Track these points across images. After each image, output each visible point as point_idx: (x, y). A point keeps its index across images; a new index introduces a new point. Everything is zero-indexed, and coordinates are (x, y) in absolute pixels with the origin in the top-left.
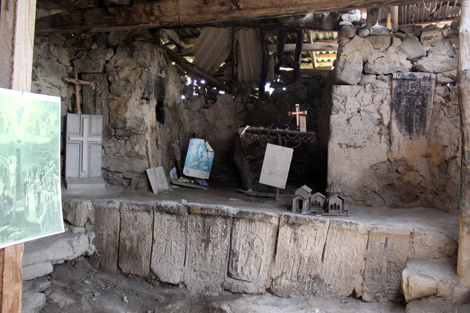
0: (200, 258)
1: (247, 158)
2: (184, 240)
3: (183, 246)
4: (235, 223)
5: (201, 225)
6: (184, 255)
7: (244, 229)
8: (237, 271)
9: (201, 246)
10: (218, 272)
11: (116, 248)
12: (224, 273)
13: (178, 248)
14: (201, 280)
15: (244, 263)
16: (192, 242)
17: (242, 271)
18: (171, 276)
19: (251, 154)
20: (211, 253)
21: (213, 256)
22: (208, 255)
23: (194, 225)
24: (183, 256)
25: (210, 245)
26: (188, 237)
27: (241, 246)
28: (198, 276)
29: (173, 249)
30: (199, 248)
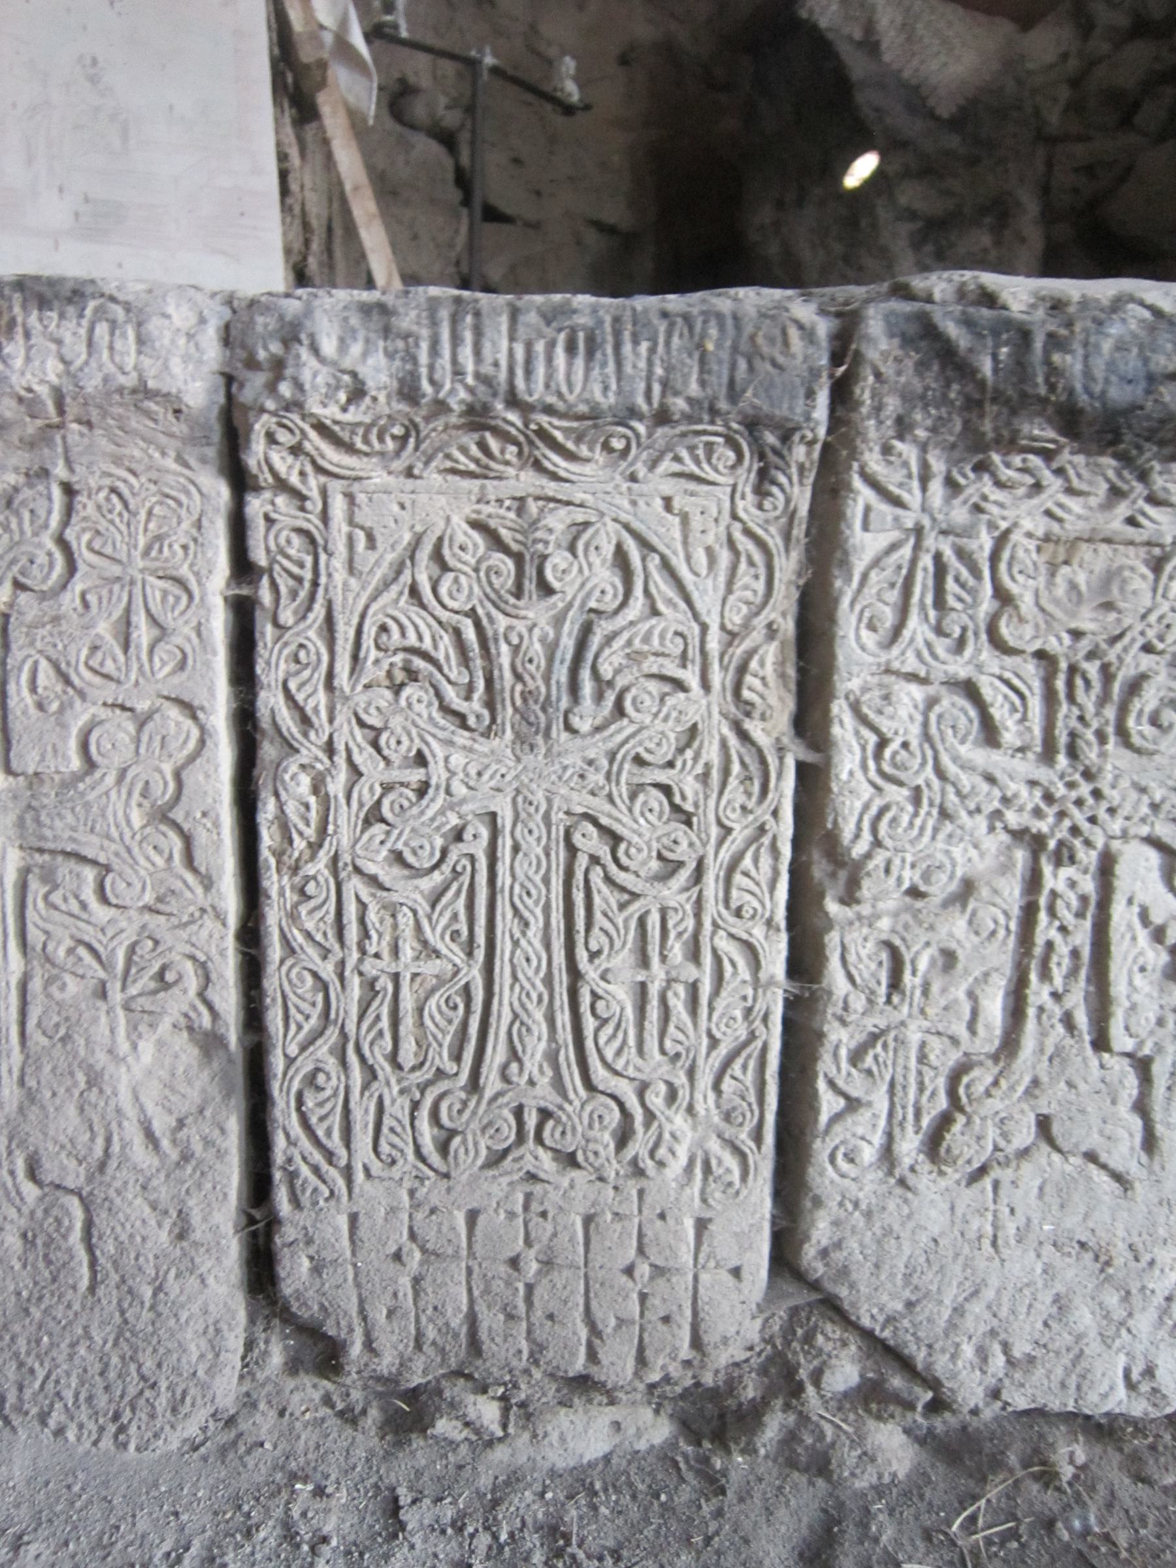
1: (903, 200)
11: (210, 1043)
18: (1114, 1328)
29: (1135, 960)
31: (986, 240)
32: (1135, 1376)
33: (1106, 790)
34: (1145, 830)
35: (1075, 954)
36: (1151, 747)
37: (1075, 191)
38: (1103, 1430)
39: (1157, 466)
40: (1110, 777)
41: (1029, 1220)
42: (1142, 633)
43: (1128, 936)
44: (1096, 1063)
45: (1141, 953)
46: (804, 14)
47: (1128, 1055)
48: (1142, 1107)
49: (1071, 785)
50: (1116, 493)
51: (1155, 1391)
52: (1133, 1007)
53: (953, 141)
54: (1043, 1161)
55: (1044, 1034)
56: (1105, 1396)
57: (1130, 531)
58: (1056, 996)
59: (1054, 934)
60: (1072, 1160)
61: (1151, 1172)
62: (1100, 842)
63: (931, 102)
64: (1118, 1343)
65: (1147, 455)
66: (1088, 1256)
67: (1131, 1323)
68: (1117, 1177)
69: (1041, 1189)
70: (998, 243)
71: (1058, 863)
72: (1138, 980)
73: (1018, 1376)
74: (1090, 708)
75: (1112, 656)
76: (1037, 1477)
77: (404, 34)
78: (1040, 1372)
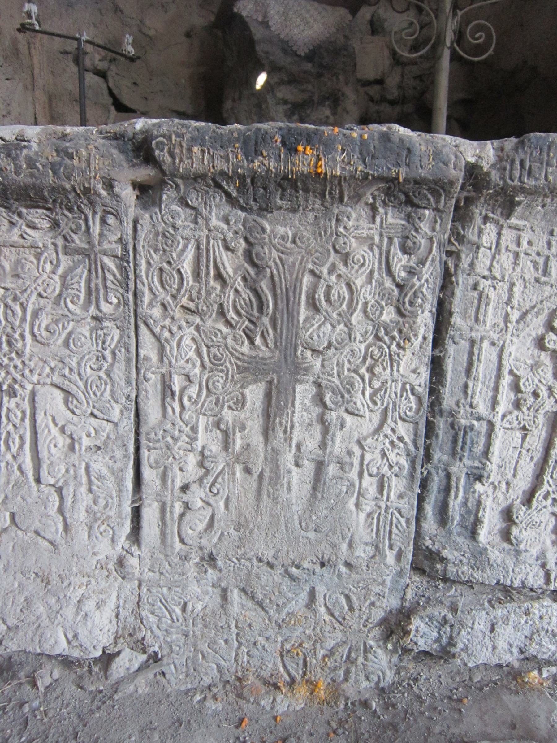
0: (239, 485)
1: (280, 95)
2: (119, 373)
3: (116, 414)
4: (471, 235)
5: (229, 264)
6: (130, 473)
7: (530, 274)
8: (473, 534)
9: (241, 403)
10: (362, 553)
12: (399, 557)
13: (87, 431)
14: (255, 616)
15: (523, 483)
16: (177, 383)
17: (506, 535)
18: (54, 614)
19: (290, 82)
20: (311, 444)
21: (320, 466)
22: (288, 458)
23: (187, 267)
24: (120, 482)
25: (304, 392)
26: (149, 349)
27: (507, 380)
28: (235, 595)
29: (53, 443)
30: (228, 415)
31: (328, 112)
32: (70, 636)
33: (27, 362)
34: (49, 381)
35: (21, 437)
36: (46, 341)
37: (415, 88)
38: (66, 662)
39: (24, 211)
40: (28, 355)
41: (8, 562)
42: (36, 289)
43: (46, 431)
44: (36, 489)
45: (55, 438)
46: (235, 10)
47: (53, 486)
48: (61, 511)
49: (11, 359)
50: (12, 224)
51: (81, 646)
52: (52, 463)
53: (308, 66)
54: (13, 535)
55: (9, 475)
56: (53, 647)
57: (22, 241)
58: (14, 457)
59: (10, 427)
60: (29, 534)
61: (67, 542)
62: (29, 387)
63: (294, 48)
64: (56, 622)
65: (15, 206)
66: (39, 580)
67: (61, 612)
68: (51, 543)
69: (13, 547)
70: (334, 114)
71: (10, 397)
72: (53, 450)
73: (11, 634)
74: (17, 323)
75: (23, 300)
76: (29, 682)
77: (37, 28)
78: (21, 633)
